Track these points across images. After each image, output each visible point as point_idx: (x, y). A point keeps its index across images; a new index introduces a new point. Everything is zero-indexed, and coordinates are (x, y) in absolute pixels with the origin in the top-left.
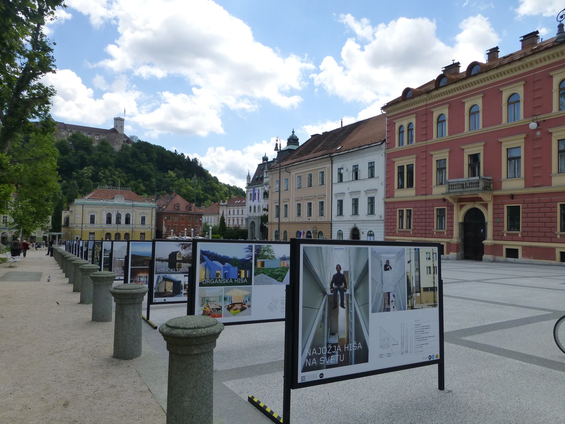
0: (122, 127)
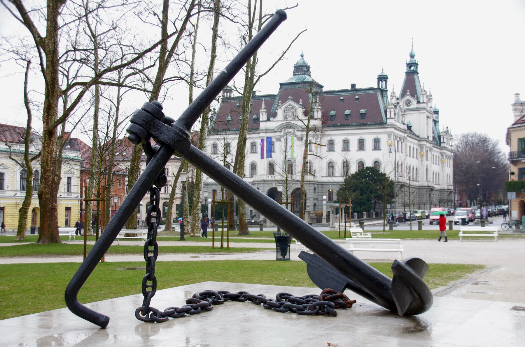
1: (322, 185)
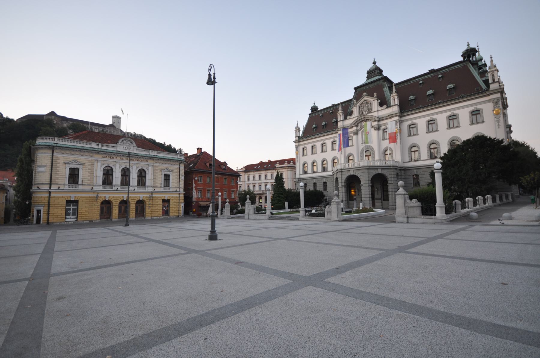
0: (119, 123)
1: (404, 170)
